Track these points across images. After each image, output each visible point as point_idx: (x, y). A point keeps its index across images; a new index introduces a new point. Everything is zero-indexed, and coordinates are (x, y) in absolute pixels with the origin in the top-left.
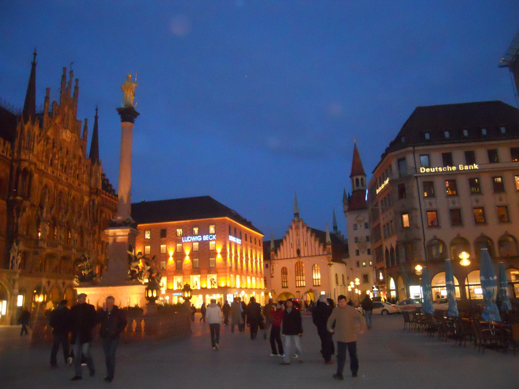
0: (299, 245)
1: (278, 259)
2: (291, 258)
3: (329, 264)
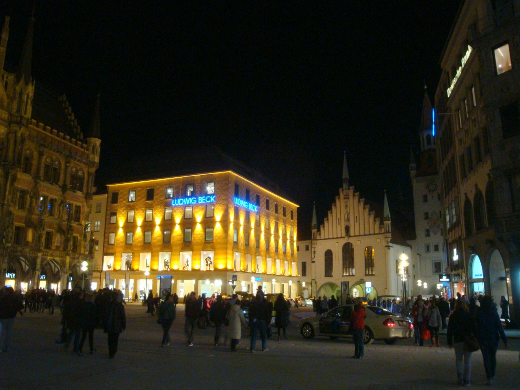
0: (348, 220)
1: (321, 239)
2: (337, 238)
3: (386, 246)
